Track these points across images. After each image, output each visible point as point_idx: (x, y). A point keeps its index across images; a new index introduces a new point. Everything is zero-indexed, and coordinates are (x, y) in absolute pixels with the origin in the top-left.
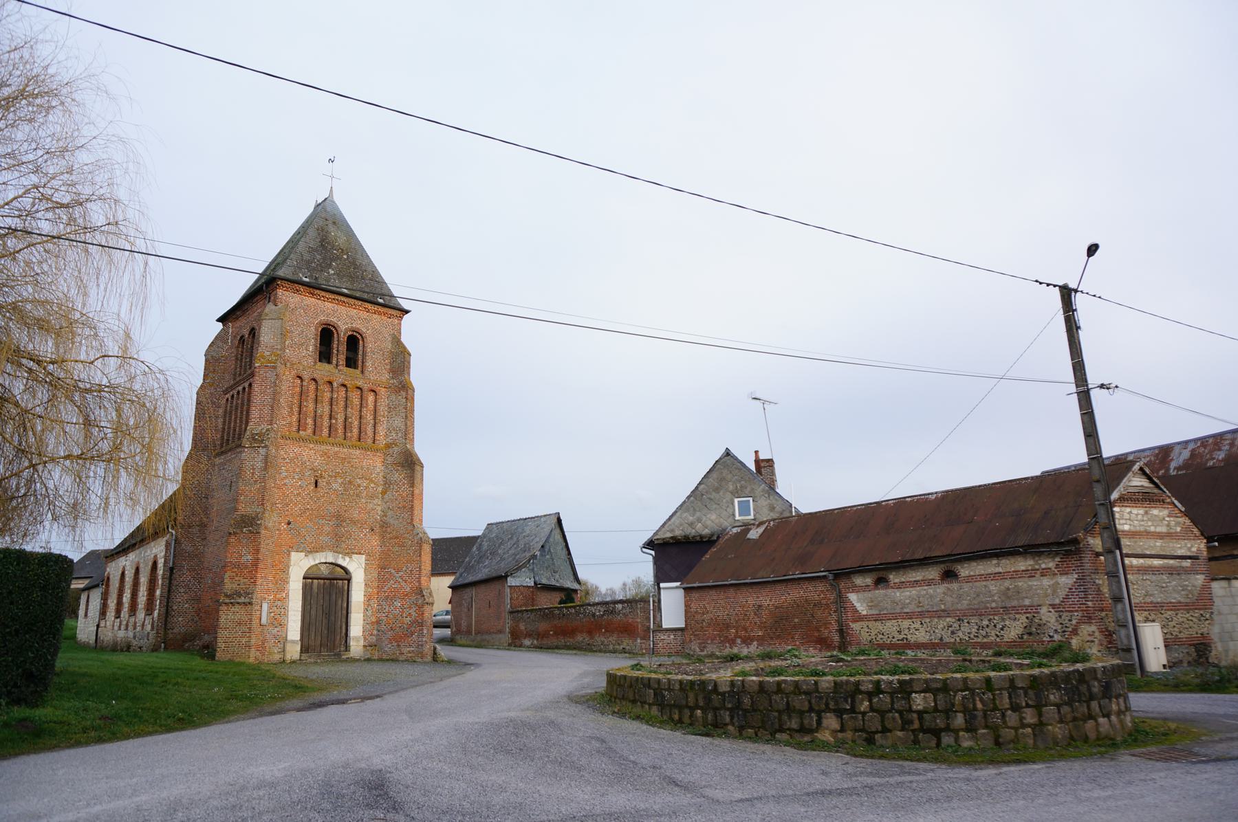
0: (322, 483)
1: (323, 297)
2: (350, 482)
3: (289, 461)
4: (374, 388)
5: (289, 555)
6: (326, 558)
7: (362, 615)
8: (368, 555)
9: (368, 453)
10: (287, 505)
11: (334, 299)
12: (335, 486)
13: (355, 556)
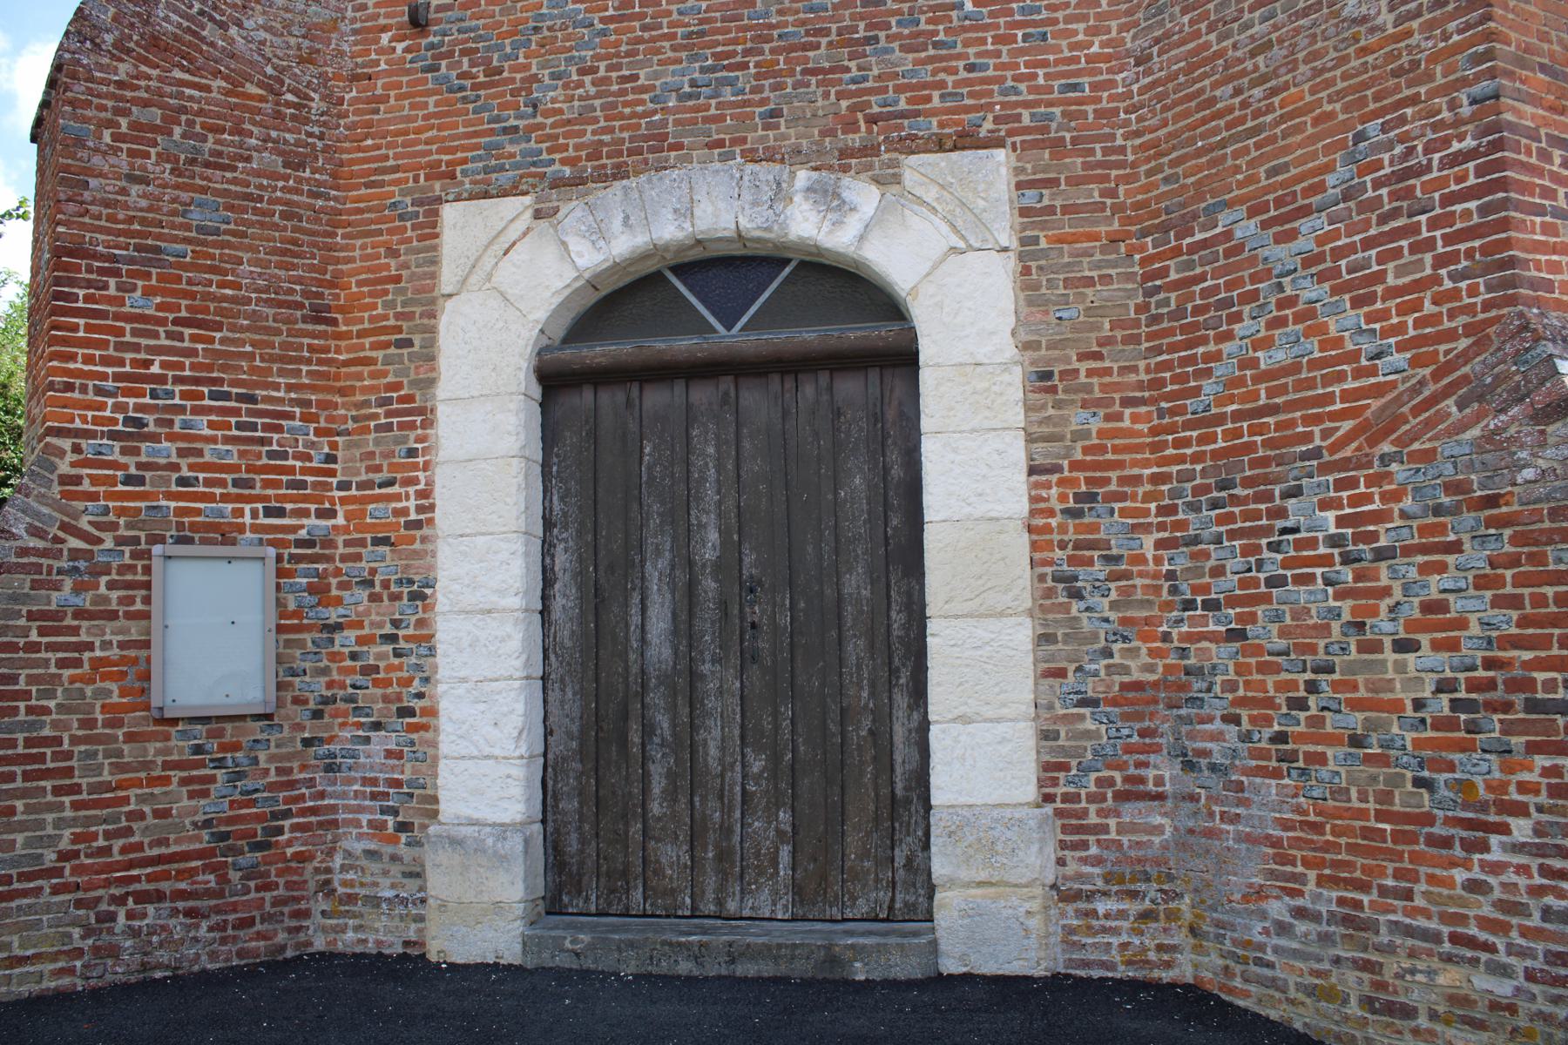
5: (430, 230)
7: (1021, 634)
8: (1040, 140)
13: (918, 169)
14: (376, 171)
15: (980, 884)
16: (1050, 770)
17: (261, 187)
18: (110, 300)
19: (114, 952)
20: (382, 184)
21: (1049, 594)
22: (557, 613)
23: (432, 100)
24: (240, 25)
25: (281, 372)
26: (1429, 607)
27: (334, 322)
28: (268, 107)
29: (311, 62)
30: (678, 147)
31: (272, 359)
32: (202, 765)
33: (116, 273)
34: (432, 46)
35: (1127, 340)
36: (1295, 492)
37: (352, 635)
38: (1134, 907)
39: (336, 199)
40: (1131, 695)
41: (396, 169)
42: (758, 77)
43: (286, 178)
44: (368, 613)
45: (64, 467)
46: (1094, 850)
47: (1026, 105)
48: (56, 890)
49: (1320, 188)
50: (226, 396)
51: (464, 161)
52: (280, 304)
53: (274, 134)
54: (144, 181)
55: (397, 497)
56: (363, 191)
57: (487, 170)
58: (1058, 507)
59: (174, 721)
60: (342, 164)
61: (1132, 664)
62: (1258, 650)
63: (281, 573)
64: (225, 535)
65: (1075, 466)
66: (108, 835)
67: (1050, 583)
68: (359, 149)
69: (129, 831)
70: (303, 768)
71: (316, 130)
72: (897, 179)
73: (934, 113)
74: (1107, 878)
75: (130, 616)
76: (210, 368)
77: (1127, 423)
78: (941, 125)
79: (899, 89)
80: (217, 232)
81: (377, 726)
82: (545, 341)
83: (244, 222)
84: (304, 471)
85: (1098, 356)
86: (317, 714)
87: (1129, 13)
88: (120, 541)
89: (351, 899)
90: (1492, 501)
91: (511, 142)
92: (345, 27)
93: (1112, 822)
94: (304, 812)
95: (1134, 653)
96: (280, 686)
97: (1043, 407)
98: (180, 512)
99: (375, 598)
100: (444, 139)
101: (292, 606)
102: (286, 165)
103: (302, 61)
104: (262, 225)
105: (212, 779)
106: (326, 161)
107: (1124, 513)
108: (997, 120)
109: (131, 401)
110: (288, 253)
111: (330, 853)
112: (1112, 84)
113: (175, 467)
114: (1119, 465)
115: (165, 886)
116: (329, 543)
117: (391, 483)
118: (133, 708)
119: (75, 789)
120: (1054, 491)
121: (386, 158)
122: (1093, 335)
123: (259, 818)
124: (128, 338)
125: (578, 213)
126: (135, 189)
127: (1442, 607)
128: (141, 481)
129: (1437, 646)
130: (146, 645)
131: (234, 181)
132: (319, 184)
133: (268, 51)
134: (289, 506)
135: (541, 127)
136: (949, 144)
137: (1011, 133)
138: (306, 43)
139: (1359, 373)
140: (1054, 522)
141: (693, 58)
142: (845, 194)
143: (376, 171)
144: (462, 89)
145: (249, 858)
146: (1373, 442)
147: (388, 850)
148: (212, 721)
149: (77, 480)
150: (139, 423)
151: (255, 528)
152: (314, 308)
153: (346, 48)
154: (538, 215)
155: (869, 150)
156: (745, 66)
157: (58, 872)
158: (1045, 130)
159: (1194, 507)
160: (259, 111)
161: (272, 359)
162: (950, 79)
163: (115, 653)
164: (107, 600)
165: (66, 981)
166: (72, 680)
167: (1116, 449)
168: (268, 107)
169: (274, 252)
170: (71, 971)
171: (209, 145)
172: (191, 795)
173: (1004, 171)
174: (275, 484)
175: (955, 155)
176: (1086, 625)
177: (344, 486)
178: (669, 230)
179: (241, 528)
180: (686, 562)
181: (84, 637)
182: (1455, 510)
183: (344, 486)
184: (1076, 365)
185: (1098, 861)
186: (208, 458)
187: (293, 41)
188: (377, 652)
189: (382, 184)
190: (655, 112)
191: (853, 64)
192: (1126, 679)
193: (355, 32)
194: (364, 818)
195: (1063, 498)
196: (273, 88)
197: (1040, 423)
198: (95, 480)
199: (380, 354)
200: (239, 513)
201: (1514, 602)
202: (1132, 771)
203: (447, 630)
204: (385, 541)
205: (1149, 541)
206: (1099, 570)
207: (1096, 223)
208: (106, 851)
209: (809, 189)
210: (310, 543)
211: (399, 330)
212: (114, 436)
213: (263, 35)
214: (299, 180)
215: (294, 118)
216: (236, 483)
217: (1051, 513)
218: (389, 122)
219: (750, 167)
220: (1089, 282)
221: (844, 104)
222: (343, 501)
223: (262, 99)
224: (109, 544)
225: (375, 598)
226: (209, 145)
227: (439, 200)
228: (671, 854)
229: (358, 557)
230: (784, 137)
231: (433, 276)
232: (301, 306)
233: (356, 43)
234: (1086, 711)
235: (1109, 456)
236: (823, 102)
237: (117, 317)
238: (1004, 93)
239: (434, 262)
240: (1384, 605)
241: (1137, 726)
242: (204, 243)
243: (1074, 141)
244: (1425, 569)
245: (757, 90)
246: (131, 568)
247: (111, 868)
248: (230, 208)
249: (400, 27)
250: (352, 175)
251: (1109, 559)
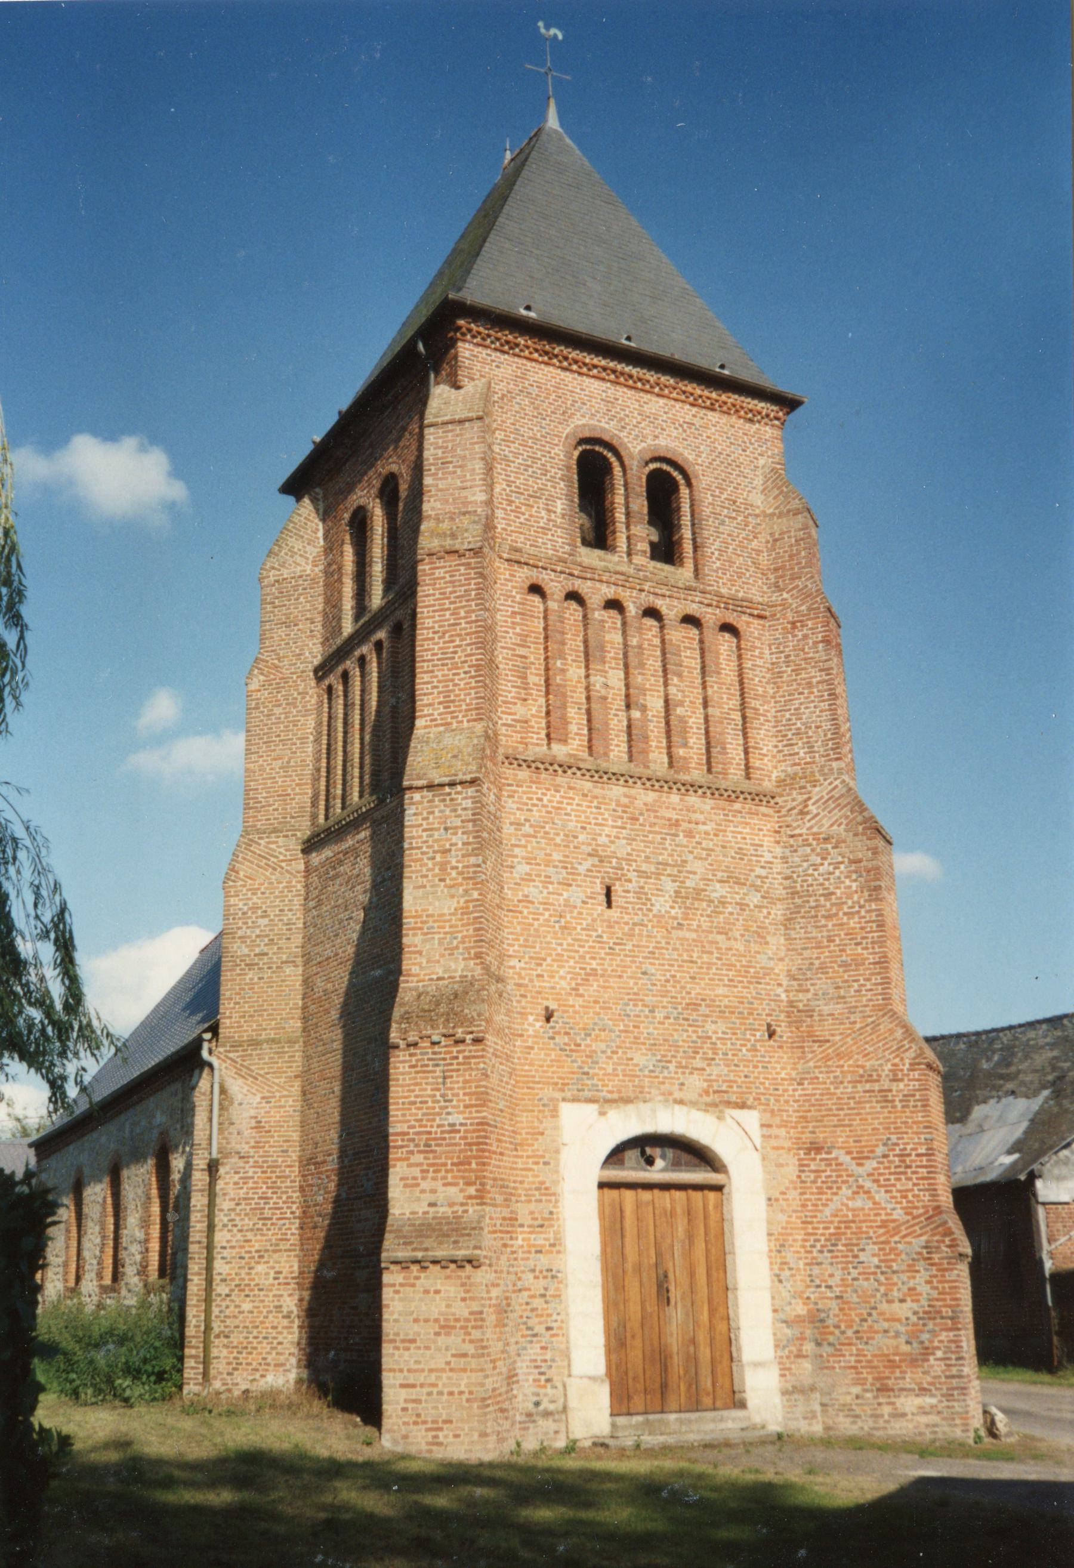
1: (576, 362)
3: (531, 831)
4: (731, 618)
5: (555, 1114)
10: (540, 961)
26: (910, 1289)
36: (863, 1250)
37: (526, 1294)
41: (539, 1083)
49: (873, 1152)
62: (848, 1303)
65: (779, 1234)
79: (724, 1081)
87: (794, 1064)
90: (929, 1259)
99: (536, 1277)
114: (791, 1234)
127: (914, 1289)
129: (913, 1301)
139: (887, 1214)
146: (892, 1236)
159: (821, 1252)
167: (791, 1228)
182: (918, 1260)
188: (537, 1303)
189: (533, 1088)
201: (936, 1288)
206: (787, 1273)
225: (536, 1277)
229: (528, 1259)
240: (895, 1289)
244: (909, 1278)
245: (676, 1073)
249: (537, 1015)
251: (790, 1269)
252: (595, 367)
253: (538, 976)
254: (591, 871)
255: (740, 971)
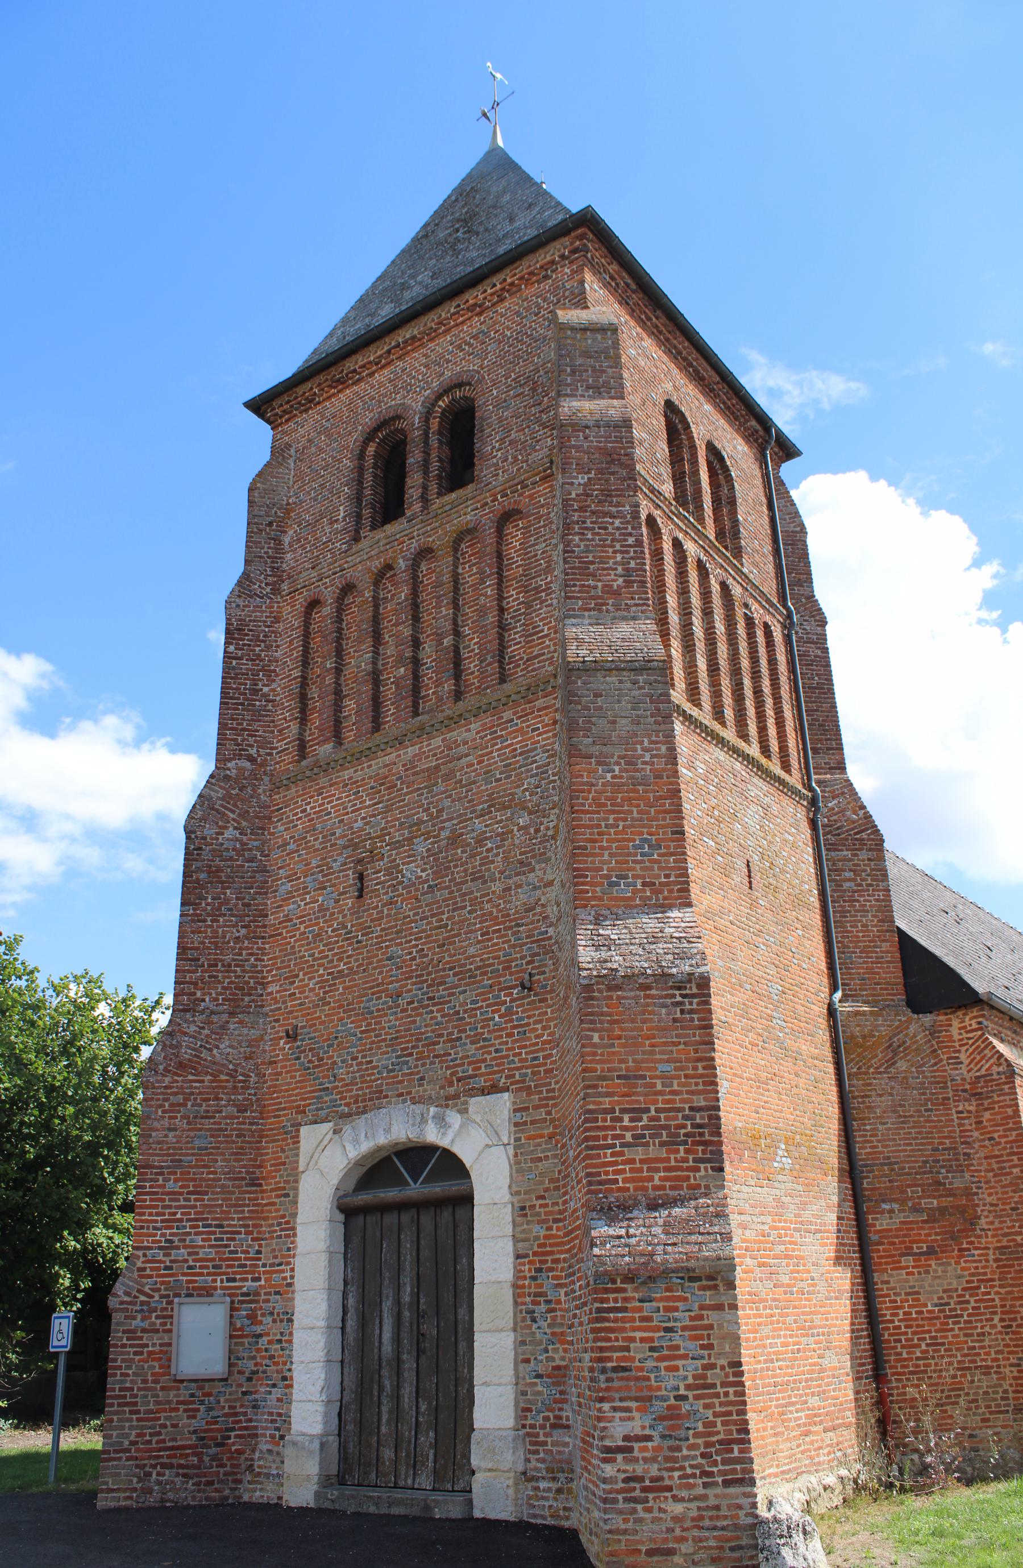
0: (377, 877)
2: (455, 840)
6: (387, 1130)
9: (507, 715)
11: (389, 352)
12: (411, 871)
13: (476, 1104)
14: (277, 1110)
15: (490, 1470)
16: (523, 1411)
17: (227, 1124)
18: (160, 1186)
19: (150, 1491)
20: (279, 1116)
21: (524, 1319)
22: (348, 1329)
23: (298, 1074)
24: (218, 1047)
25: (236, 1212)
27: (260, 1185)
28: (230, 1085)
29: (251, 1058)
30: (386, 1097)
31: (231, 1206)
32: (194, 1403)
33: (162, 1174)
34: (298, 1047)
35: (557, 1188)
37: (265, 1339)
38: (554, 1486)
39: (262, 1124)
40: (556, 1372)
41: (284, 1109)
42: (417, 1059)
43: (238, 1118)
44: (271, 1328)
45: (139, 1264)
46: (542, 1455)
47: (518, 1069)
48: (128, 1459)
50: (210, 1226)
51: (309, 1105)
52: (235, 1179)
53: (233, 1097)
54: (175, 1130)
55: (283, 1271)
56: (273, 1120)
57: (318, 1109)
58: (528, 1275)
59: (182, 1381)
60: (265, 1106)
61: (556, 1356)
63: (232, 1309)
64: (207, 1292)
65: (535, 1254)
66: (151, 1435)
67: (524, 1314)
68: (272, 1099)
69: (159, 1433)
70: (242, 1406)
71: (253, 1092)
72: (466, 1111)
73: (482, 1075)
74: (548, 1470)
75: (165, 1331)
76: (202, 1213)
77: (554, 1232)
78: (485, 1081)
80: (206, 1148)
81: (274, 1386)
82: (341, 1193)
83: (219, 1142)
84: (246, 1259)
85: (543, 1197)
86: (249, 1379)
88: (162, 1296)
89: (259, 1474)
91: (327, 1095)
92: (267, 1038)
93: (549, 1440)
94: (241, 1429)
95: (556, 1350)
96: (230, 1365)
97: (522, 1224)
98: (188, 1282)
100: (303, 1094)
101: (238, 1325)
102: (239, 1111)
103: (246, 1058)
104: (227, 1142)
105: (198, 1410)
106: (258, 1106)
107: (554, 1278)
108: (507, 1077)
109: (168, 1231)
110: (238, 1155)
111: (253, 1451)
112: (551, 1055)
113: (186, 1261)
114: (552, 1253)
115: (174, 1461)
116: (258, 1294)
117: (280, 1264)
118: (164, 1374)
119: (138, 1412)
120: (527, 1267)
121: (281, 1103)
122: (542, 1187)
123: (219, 1430)
124: (167, 1203)
125: (349, 1131)
126: (171, 1134)
128: (171, 1268)
130: (170, 1345)
131: (214, 1123)
132: (254, 1118)
133: (230, 1057)
134: (238, 1277)
135: (337, 1087)
136: (486, 1092)
137: (512, 1084)
138: (249, 1049)
140: (527, 1282)
141: (394, 1051)
142: (447, 1119)
143: (277, 1110)
144: (309, 1068)
145: (214, 1450)
147: (275, 1449)
148: (200, 1382)
149: (144, 1269)
150: (171, 1241)
151: (222, 1288)
152: (251, 1179)
153: (267, 1048)
154: (335, 1132)
155: (456, 1096)
156: (411, 1054)
157: (129, 1450)
158: (524, 1081)
160: (226, 1087)
161: (231, 1206)
162: (488, 1057)
163: (157, 1348)
164: (154, 1324)
165: (129, 1502)
166: (140, 1361)
167: (551, 1245)
168: (230, 1085)
169: (233, 1154)
170: (130, 1498)
171: (204, 1108)
172: (189, 1417)
173: (508, 1104)
174: (232, 1266)
175: (488, 1097)
176: (538, 1336)
177: (264, 1266)
178: (382, 1140)
179: (215, 1288)
180: (398, 1302)
181: (145, 1341)
183: (264, 1266)
184: (535, 1202)
185: (543, 1461)
186: (201, 1256)
187: (242, 1050)
189: (279, 1116)
190: (378, 1079)
191: (452, 1052)
192: (554, 1364)
193: (271, 1040)
194: (268, 1432)
195: (530, 1270)
196: (233, 1074)
197: (521, 1233)
198: (152, 1269)
199: (277, 1200)
200: (215, 1281)
202: (557, 1413)
203: (298, 1337)
204: (277, 1293)
205: (562, 1291)
206: (543, 1307)
207: (542, 1129)
208: (150, 1442)
209: (434, 1117)
210: (247, 1294)
211: (284, 1188)
212: (160, 1248)
213: (229, 1050)
214: (244, 1118)
215: (242, 1087)
216: (214, 1267)
217: (525, 1278)
218: (282, 1085)
219: (412, 1106)
220: (540, 1159)
221: (448, 1072)
222: (264, 1272)
223: (227, 1081)
224: (157, 1298)
225: (274, 1321)
226: (204, 1108)
227: (300, 1125)
228: (388, 1453)
230: (425, 1091)
231: (297, 1162)
232: (244, 1179)
233: (271, 1045)
234: (538, 1381)
235: (548, 1249)
236: (441, 1072)
237: (163, 1194)
238: (509, 1063)
239: (298, 1155)
241: (559, 1389)
242: (201, 1155)
243: (535, 1086)
245: (416, 1066)
246: (166, 1309)
247: (150, 1450)
248: (212, 1136)
250: (269, 1111)
251: (548, 1302)
252: (381, 356)
253: (290, 995)
254: (345, 864)
255: (497, 917)
